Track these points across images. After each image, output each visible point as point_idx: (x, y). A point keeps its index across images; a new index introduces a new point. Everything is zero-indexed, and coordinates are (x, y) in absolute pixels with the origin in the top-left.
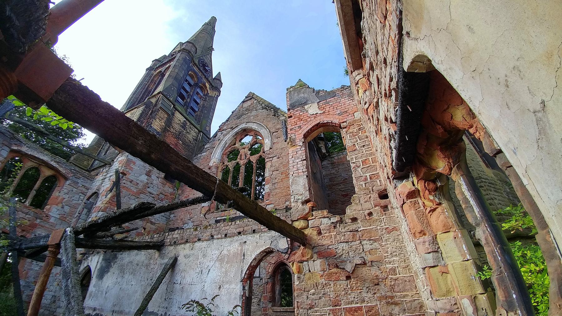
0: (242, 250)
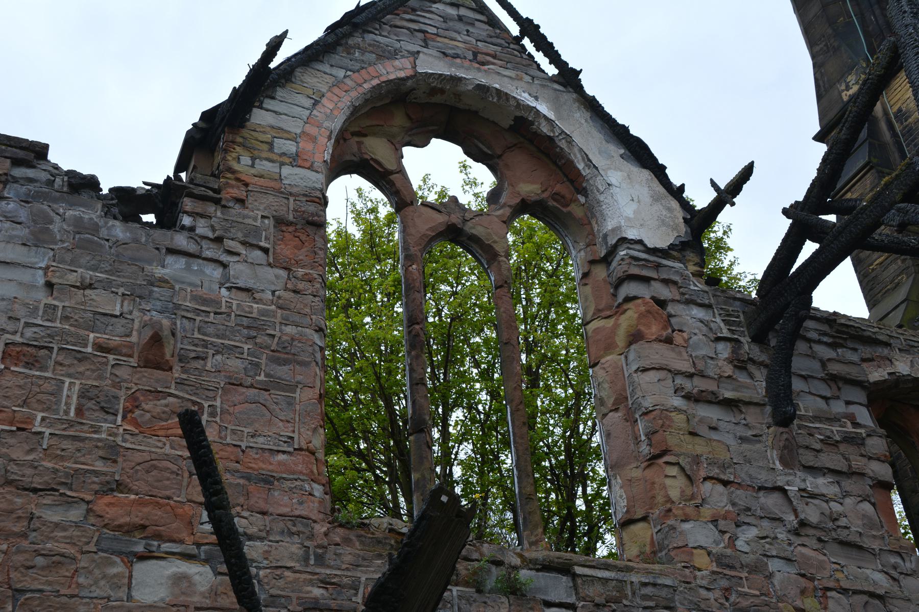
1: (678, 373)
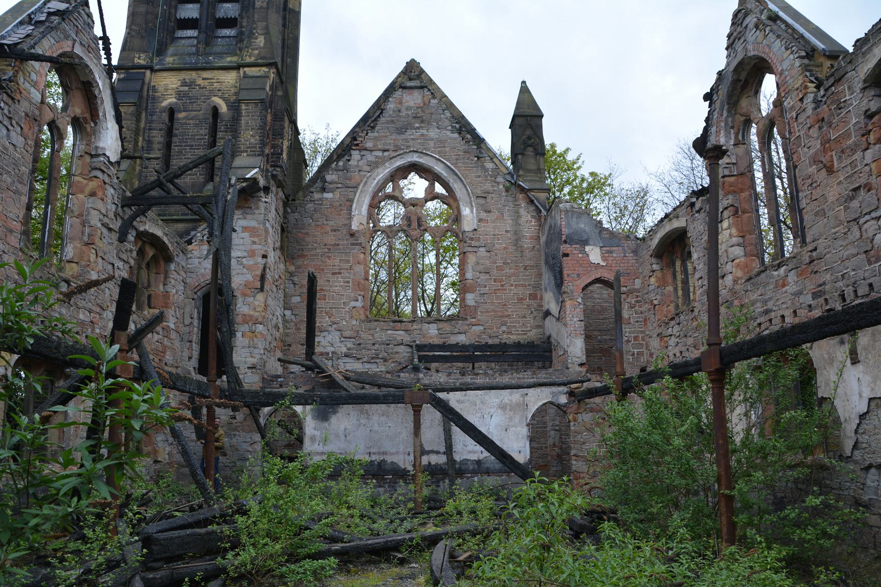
0: (524, 400)
1: (102, 214)
